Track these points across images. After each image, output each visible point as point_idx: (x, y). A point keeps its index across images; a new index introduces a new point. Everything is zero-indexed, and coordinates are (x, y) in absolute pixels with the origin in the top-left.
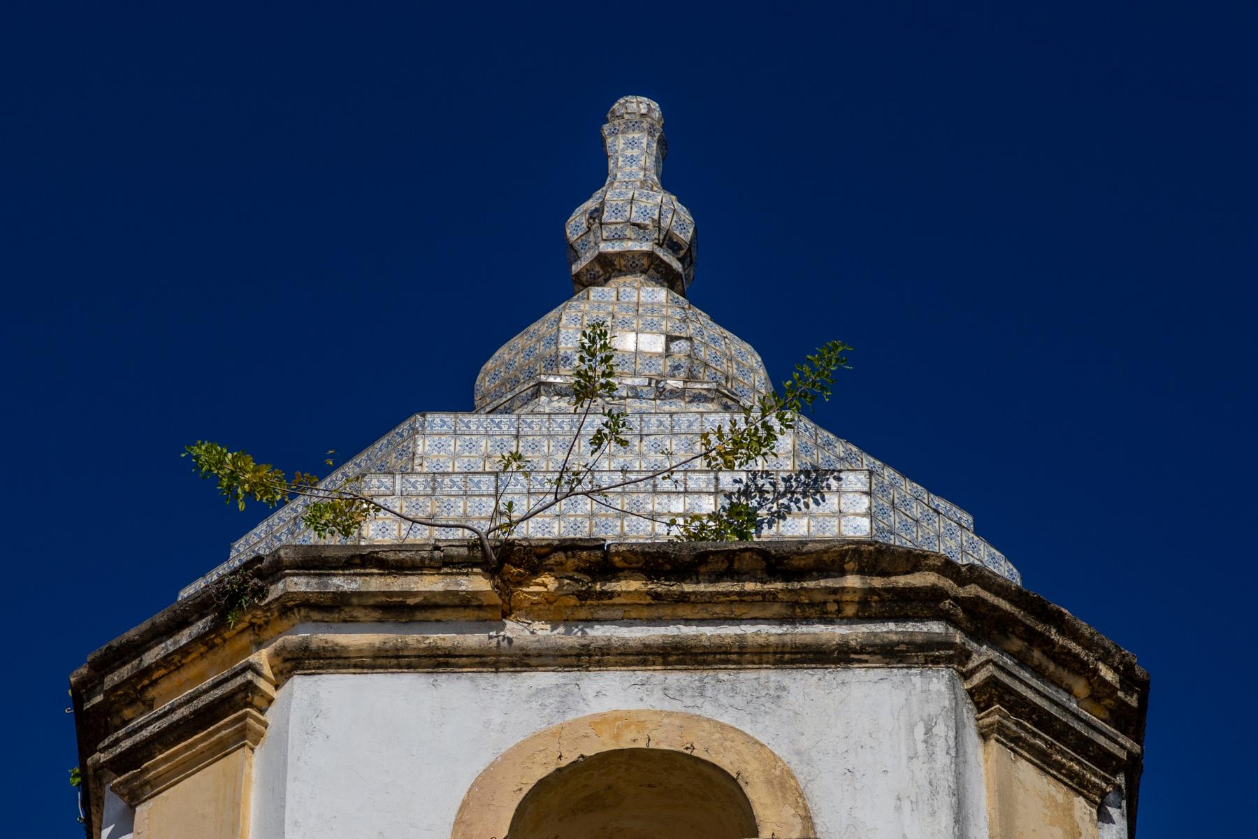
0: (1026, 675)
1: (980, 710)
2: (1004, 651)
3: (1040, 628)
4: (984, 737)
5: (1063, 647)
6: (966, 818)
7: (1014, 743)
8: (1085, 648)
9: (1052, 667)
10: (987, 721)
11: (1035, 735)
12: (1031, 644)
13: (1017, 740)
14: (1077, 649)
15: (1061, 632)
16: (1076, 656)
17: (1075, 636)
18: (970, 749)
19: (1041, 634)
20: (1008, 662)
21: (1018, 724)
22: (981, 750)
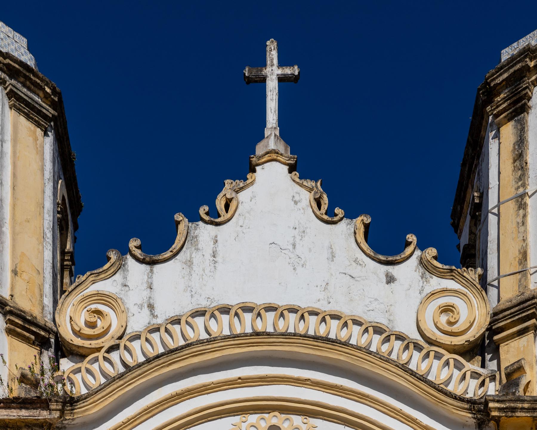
0: (25, 90)
1: (10, 100)
2: (19, 82)
3: (27, 74)
4: (11, 108)
5: (34, 81)
6: (4, 133)
7: (19, 110)
8: (41, 81)
9: (33, 87)
10: (11, 103)
11: (24, 108)
12: (26, 79)
13: (19, 109)
14: (39, 81)
15: (34, 76)
16: (39, 84)
17: (38, 77)
18: (6, 112)
19: (28, 76)
20: (19, 86)
21: (19, 104)
22: (10, 112)
